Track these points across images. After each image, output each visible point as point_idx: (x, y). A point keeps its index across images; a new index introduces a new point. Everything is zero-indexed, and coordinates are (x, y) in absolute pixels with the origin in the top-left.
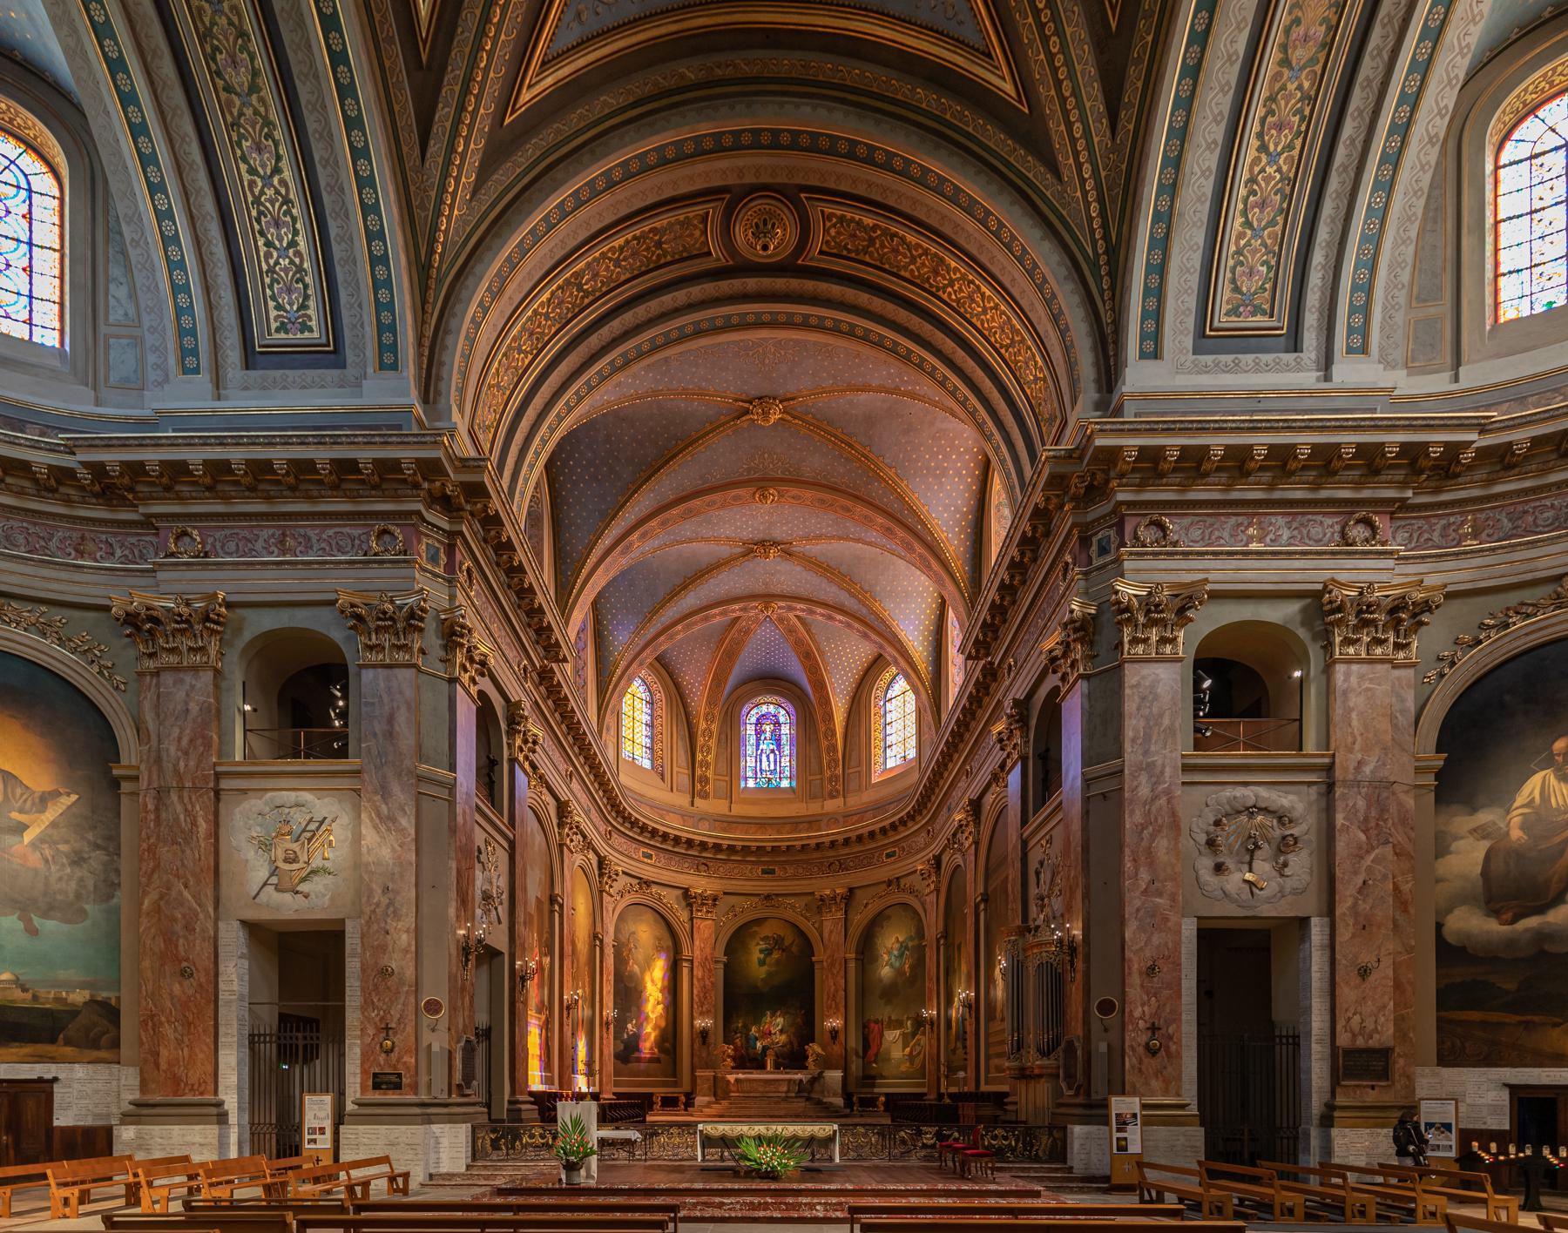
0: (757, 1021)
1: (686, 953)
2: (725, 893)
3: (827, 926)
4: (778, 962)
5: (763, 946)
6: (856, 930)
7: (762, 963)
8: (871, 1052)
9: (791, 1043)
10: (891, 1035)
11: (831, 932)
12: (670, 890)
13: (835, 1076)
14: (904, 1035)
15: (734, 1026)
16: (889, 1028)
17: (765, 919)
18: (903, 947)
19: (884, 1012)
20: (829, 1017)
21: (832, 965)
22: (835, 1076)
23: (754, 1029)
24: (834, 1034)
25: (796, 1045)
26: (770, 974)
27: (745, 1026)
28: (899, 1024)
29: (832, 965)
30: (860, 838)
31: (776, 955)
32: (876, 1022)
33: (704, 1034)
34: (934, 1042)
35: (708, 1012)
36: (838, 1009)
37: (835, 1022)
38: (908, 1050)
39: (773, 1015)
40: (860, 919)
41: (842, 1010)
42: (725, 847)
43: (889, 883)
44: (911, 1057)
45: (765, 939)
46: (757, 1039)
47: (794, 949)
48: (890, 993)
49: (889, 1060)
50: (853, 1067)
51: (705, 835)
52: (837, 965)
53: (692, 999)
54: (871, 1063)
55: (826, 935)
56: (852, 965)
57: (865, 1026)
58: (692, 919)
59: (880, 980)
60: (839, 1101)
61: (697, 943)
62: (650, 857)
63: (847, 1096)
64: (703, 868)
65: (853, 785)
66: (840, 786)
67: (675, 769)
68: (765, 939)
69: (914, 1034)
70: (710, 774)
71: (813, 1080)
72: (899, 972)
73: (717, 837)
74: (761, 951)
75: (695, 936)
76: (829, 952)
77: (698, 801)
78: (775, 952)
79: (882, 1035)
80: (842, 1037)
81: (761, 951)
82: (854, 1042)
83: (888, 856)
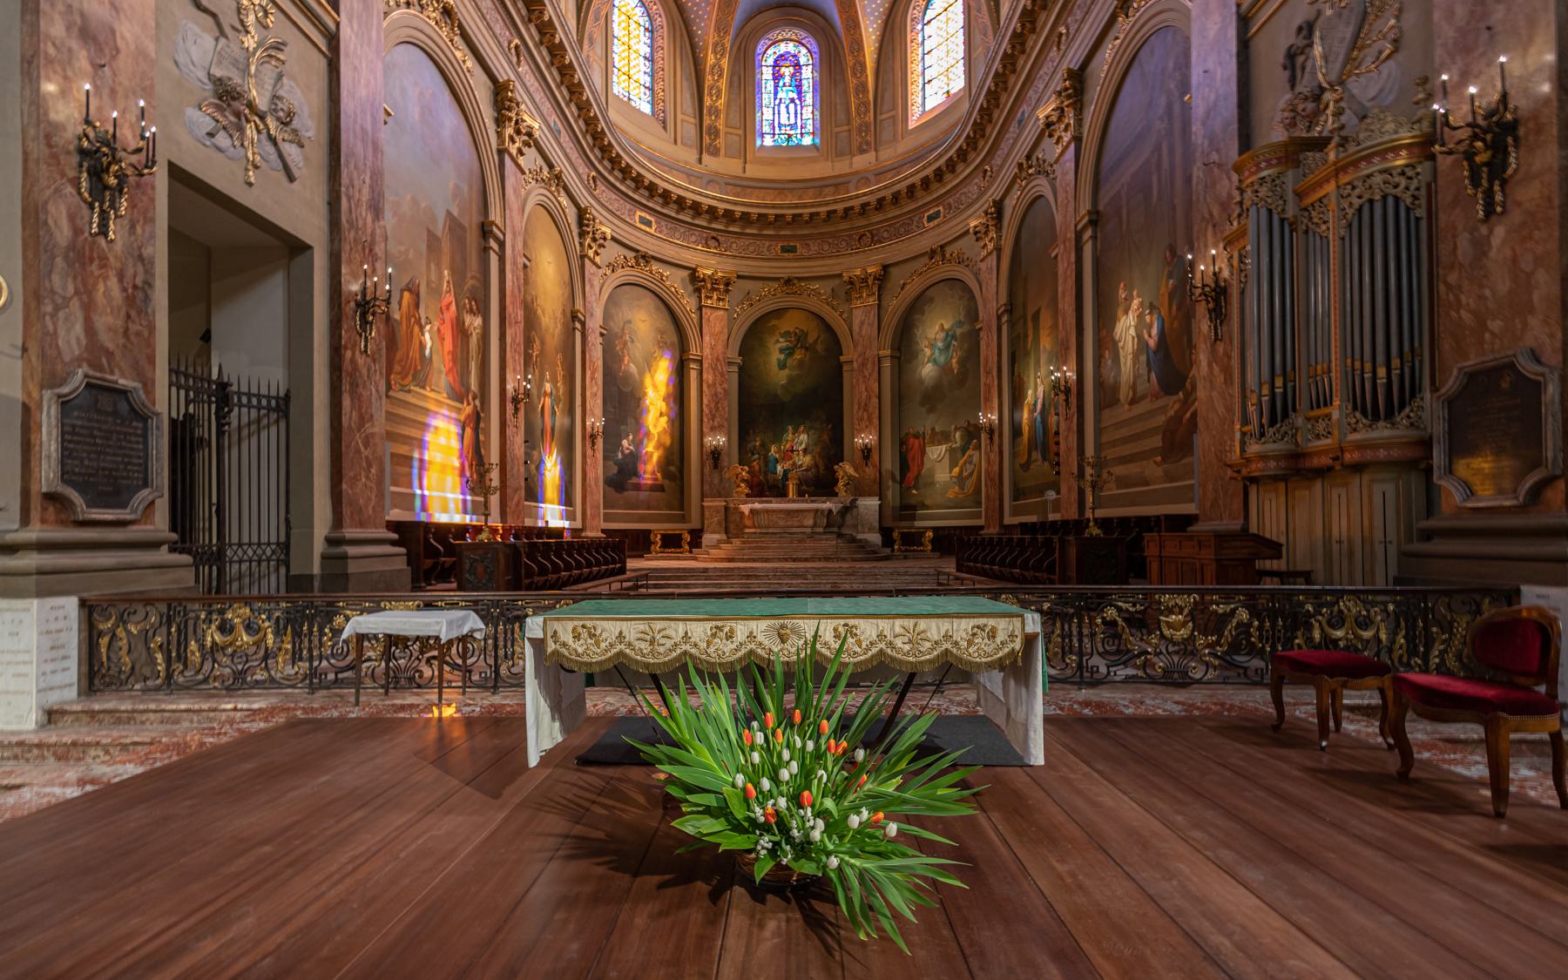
0: (777, 439)
1: (694, 352)
2: (739, 277)
3: (858, 316)
4: (801, 363)
5: (783, 344)
7: (782, 366)
8: (911, 476)
9: (816, 466)
10: (936, 452)
11: (862, 323)
12: (674, 270)
13: (869, 504)
14: (951, 451)
16: (933, 443)
17: (786, 309)
19: (925, 422)
20: (860, 431)
21: (864, 365)
22: (869, 504)
23: (773, 449)
24: (866, 452)
25: (822, 468)
26: (791, 380)
27: (763, 445)
28: (945, 437)
29: (864, 365)
30: (896, 198)
31: (798, 356)
32: (916, 436)
33: (716, 454)
34: (994, 457)
35: (721, 426)
36: (870, 419)
37: (866, 439)
38: (956, 470)
39: (795, 431)
40: (895, 304)
41: (876, 421)
42: (738, 215)
44: (961, 479)
45: (786, 334)
46: (777, 461)
47: (819, 347)
48: (933, 397)
49: (933, 484)
50: (889, 494)
51: (714, 198)
52: (869, 365)
53: (702, 411)
54: (909, 488)
55: (856, 328)
56: (887, 364)
57: (902, 443)
58: (700, 308)
59: (921, 382)
60: (875, 538)
61: (707, 338)
62: (649, 224)
63: (886, 532)
64: (712, 243)
65: (886, 135)
66: (869, 137)
67: (679, 116)
68: (786, 334)
69: (964, 449)
70: (721, 125)
71: (847, 510)
73: (728, 202)
74: (781, 351)
75: (705, 330)
76: (859, 349)
77: (705, 157)
78: (798, 351)
79: (923, 453)
80: (875, 457)
81: (781, 351)
82: (889, 463)
83: (930, 219)
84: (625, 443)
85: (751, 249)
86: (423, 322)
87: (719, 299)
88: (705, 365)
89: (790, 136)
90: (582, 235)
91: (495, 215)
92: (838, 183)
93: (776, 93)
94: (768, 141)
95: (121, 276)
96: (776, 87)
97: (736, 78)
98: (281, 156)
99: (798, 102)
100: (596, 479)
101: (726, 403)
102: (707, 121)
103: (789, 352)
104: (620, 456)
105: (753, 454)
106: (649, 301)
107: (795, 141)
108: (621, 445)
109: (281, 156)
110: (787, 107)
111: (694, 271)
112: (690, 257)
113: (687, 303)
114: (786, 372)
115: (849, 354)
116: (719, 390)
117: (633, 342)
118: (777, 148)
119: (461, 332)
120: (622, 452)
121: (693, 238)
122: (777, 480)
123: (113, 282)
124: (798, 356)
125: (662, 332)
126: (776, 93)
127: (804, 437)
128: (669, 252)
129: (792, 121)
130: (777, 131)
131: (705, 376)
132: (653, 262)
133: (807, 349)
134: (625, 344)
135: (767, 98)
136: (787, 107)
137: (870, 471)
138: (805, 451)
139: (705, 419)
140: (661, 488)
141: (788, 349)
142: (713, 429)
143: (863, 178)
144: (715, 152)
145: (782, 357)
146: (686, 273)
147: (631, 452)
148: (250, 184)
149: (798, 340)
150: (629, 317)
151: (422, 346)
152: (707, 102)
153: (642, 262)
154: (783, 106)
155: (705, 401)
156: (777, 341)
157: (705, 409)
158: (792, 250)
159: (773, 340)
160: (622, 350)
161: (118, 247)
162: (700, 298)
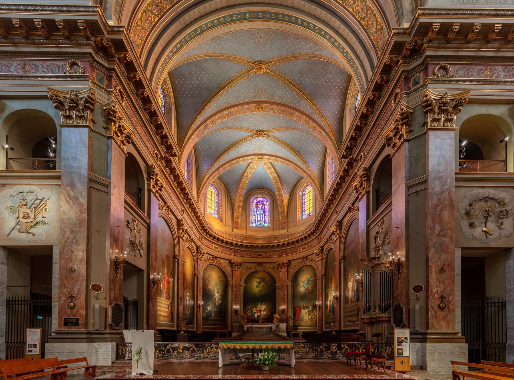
0: (255, 307)
3: (281, 274)
4: (263, 286)
5: (258, 280)
6: (291, 275)
7: (257, 287)
10: (304, 312)
13: (283, 326)
18: (309, 280)
21: (283, 287)
22: (283, 326)
24: (283, 311)
26: (260, 291)
28: (307, 307)
31: (262, 284)
33: (236, 311)
37: (283, 307)
43: (304, 258)
44: (311, 319)
56: (290, 287)
60: (285, 334)
72: (307, 289)
82: (290, 314)
92: (276, 238)
102: (235, 220)
111: (230, 261)
115: (278, 284)
137: (284, 316)
143: (283, 236)
144: (237, 228)
152: (235, 214)
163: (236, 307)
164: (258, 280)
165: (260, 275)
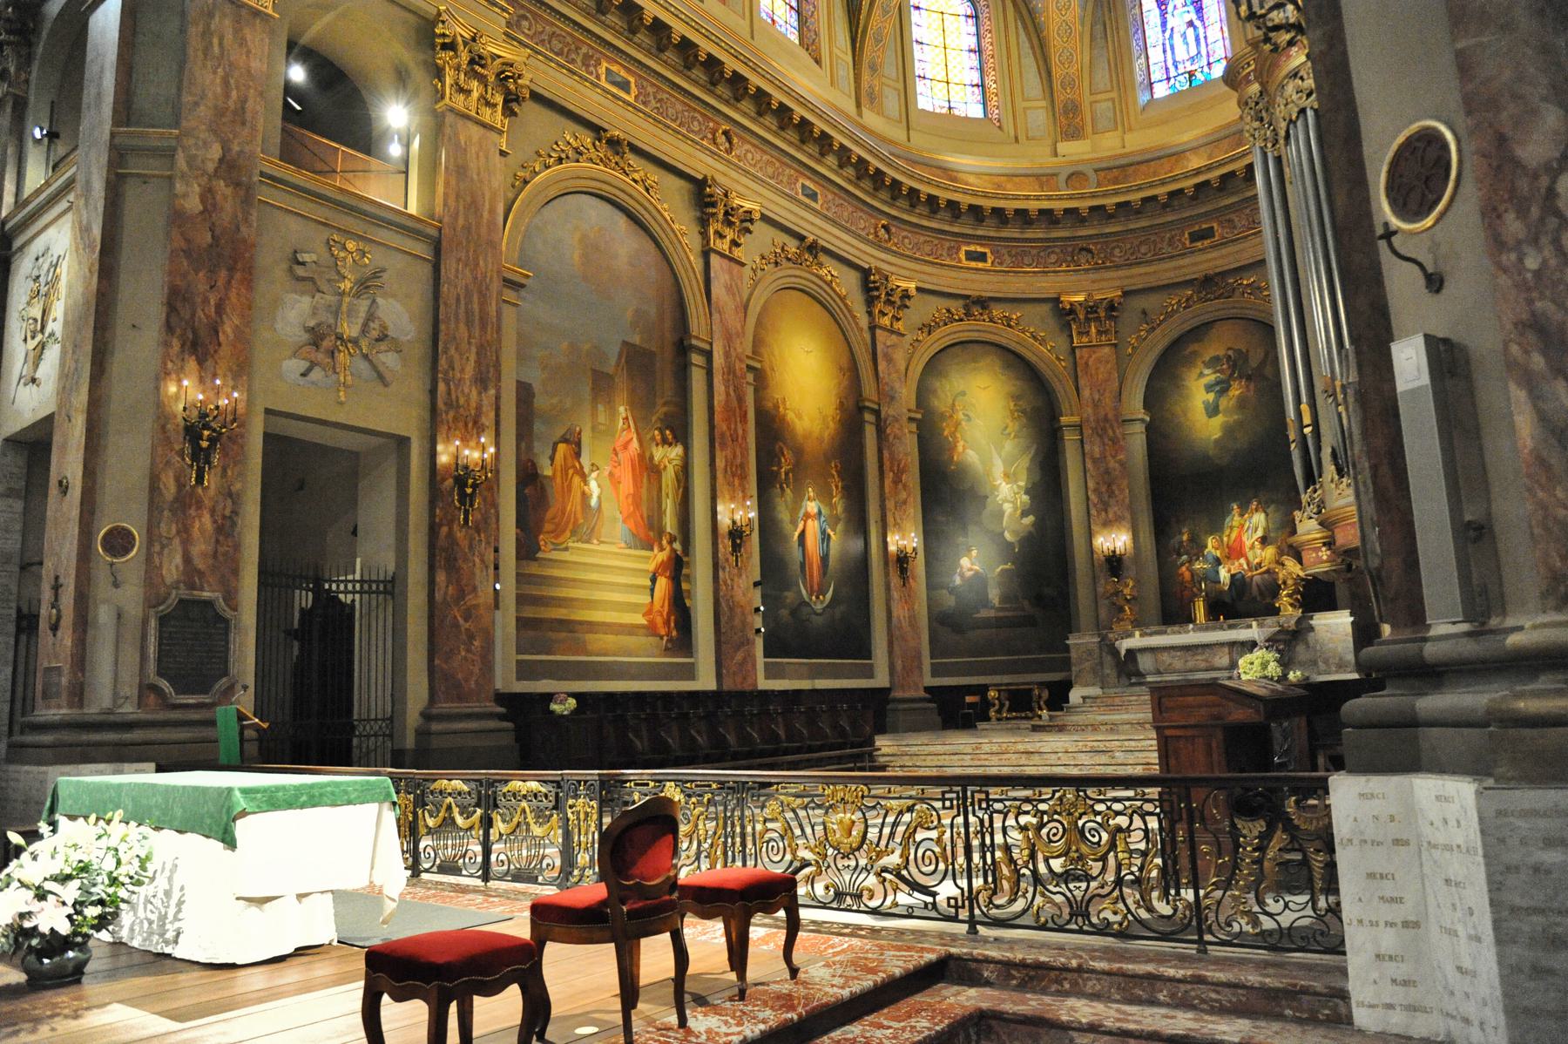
0: (1217, 527)
2: (1126, 294)
4: (1242, 403)
5: (1210, 376)
7: (1212, 411)
12: (1029, 308)
15: (1174, 542)
17: (1208, 325)
23: (1211, 542)
26: (1229, 431)
27: (1192, 539)
31: (1236, 391)
51: (1071, 197)
58: (1073, 349)
61: (1086, 393)
64: (1084, 257)
68: (1214, 362)
74: (1209, 388)
75: (1082, 382)
78: (1235, 385)
81: (1209, 388)
84: (965, 562)
85: (1143, 249)
86: (586, 470)
87: (1099, 333)
88: (1087, 432)
89: (1191, 74)
90: (870, 302)
91: (697, 324)
93: (1164, 24)
94: (1161, 91)
95: (213, 512)
96: (1163, 14)
97: (1099, 27)
98: (374, 367)
99: (1197, 23)
100: (913, 620)
101: (1125, 482)
103: (1221, 388)
104: (958, 581)
105: (1180, 555)
106: (991, 362)
107: (1200, 77)
108: (959, 565)
109: (374, 367)
110: (1184, 36)
111: (1056, 301)
112: (1045, 285)
113: (1047, 350)
114: (1218, 421)
116: (1112, 464)
117: (969, 418)
118: (1177, 96)
119: (648, 469)
120: (962, 575)
121: (1053, 258)
122: (1222, 592)
123: (207, 519)
124: (1236, 391)
125: (1016, 398)
126: (1164, 24)
127: (1259, 519)
128: (1016, 285)
129: (1193, 51)
130: (1173, 73)
131: (1087, 448)
132: (992, 305)
133: (1249, 378)
134: (958, 424)
135: (1153, 33)
136: (1184, 36)
138: (1264, 541)
139: (1093, 512)
140: (1029, 621)
141: (1218, 383)
142: (1107, 524)
145: (1211, 397)
146: (1045, 309)
147: (977, 573)
148: (341, 403)
149: (1234, 367)
150: (962, 388)
151: (585, 497)
153: (976, 311)
154: (1177, 37)
155: (1091, 485)
156: (1201, 375)
157: (1093, 497)
158: (1207, 234)
159: (1195, 372)
160: (953, 434)
161: (212, 492)
162: (1071, 336)
163: (1115, 540)
164: (1210, 376)
165: (1215, 347)
